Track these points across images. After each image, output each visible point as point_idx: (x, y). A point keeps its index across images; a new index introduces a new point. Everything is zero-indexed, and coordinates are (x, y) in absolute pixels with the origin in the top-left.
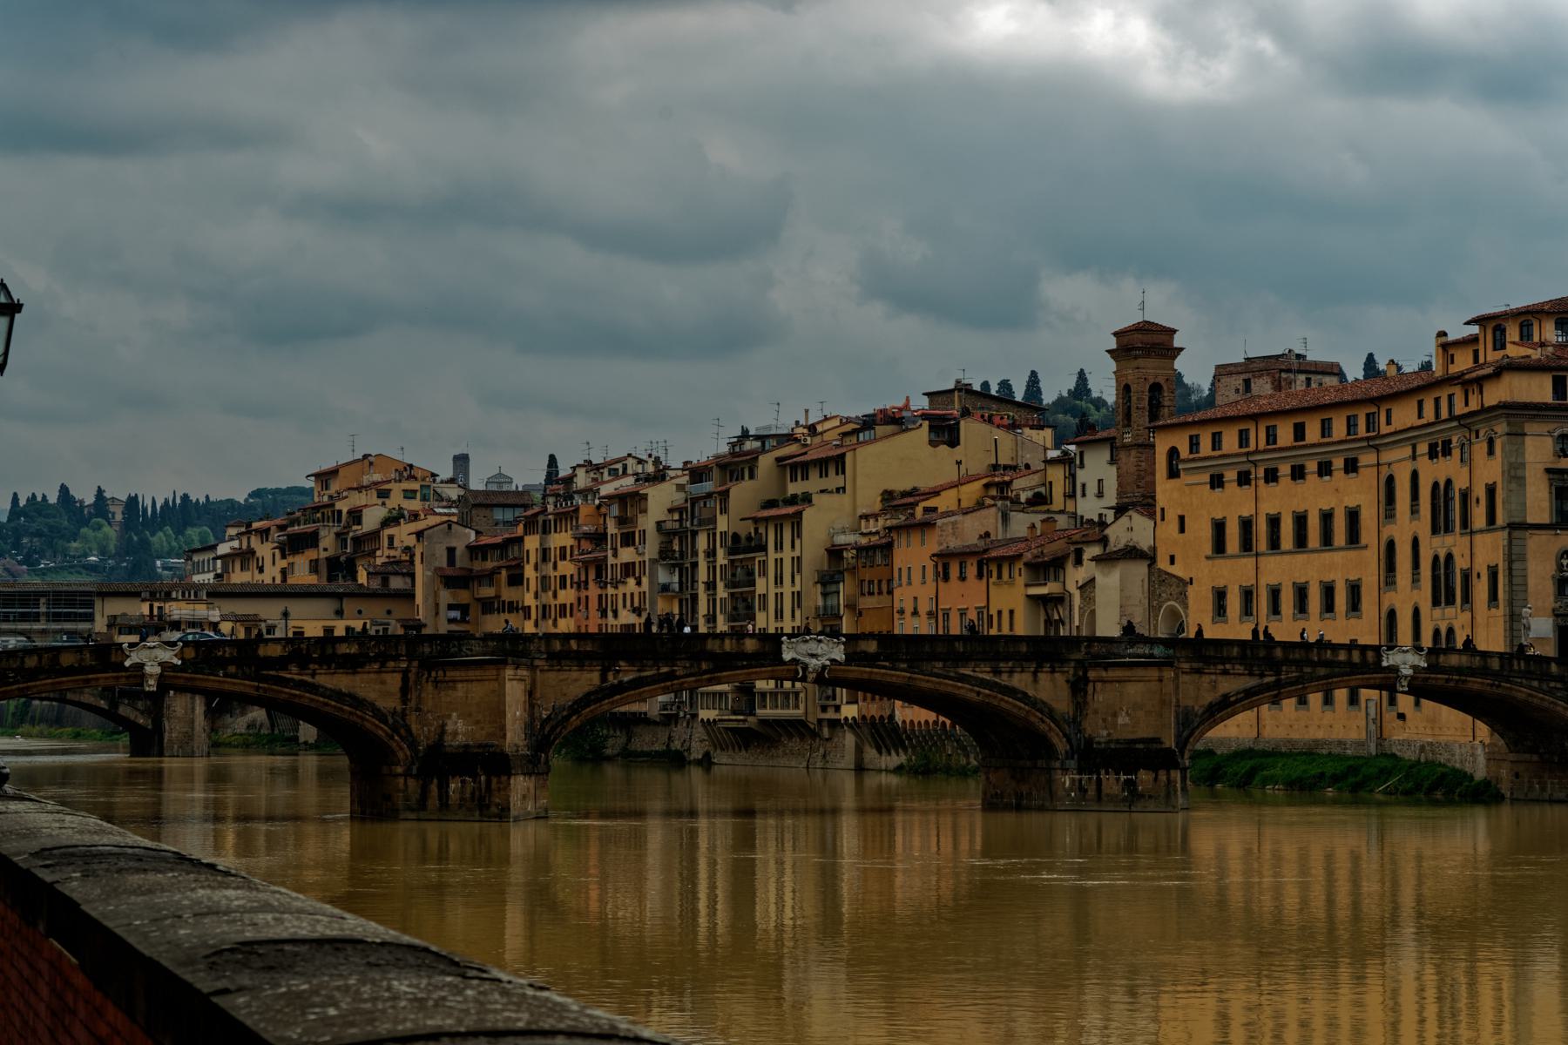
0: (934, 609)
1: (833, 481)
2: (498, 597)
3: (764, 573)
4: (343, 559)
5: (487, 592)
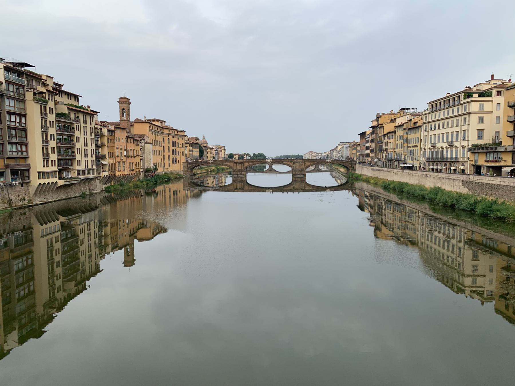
0: (126, 148)
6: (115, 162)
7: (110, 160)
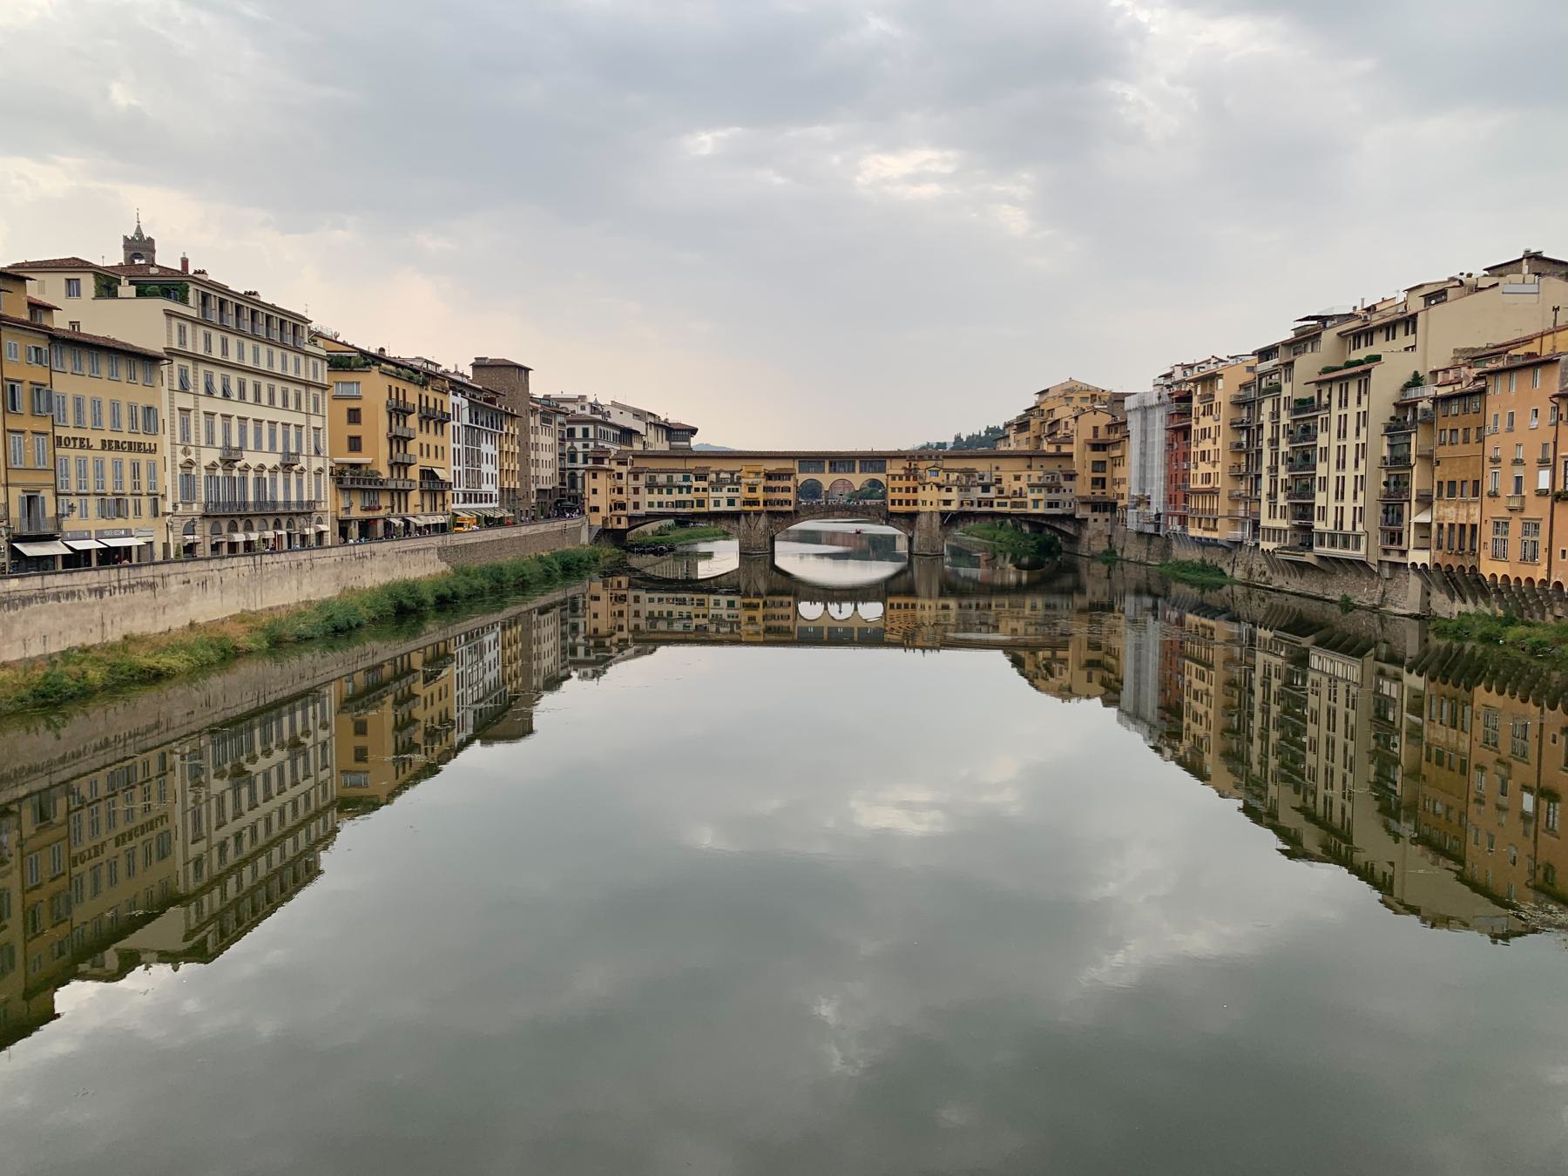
0: (1551, 456)
1: (1402, 339)
4: (1042, 437)
6: (1476, 520)
7: (1448, 510)
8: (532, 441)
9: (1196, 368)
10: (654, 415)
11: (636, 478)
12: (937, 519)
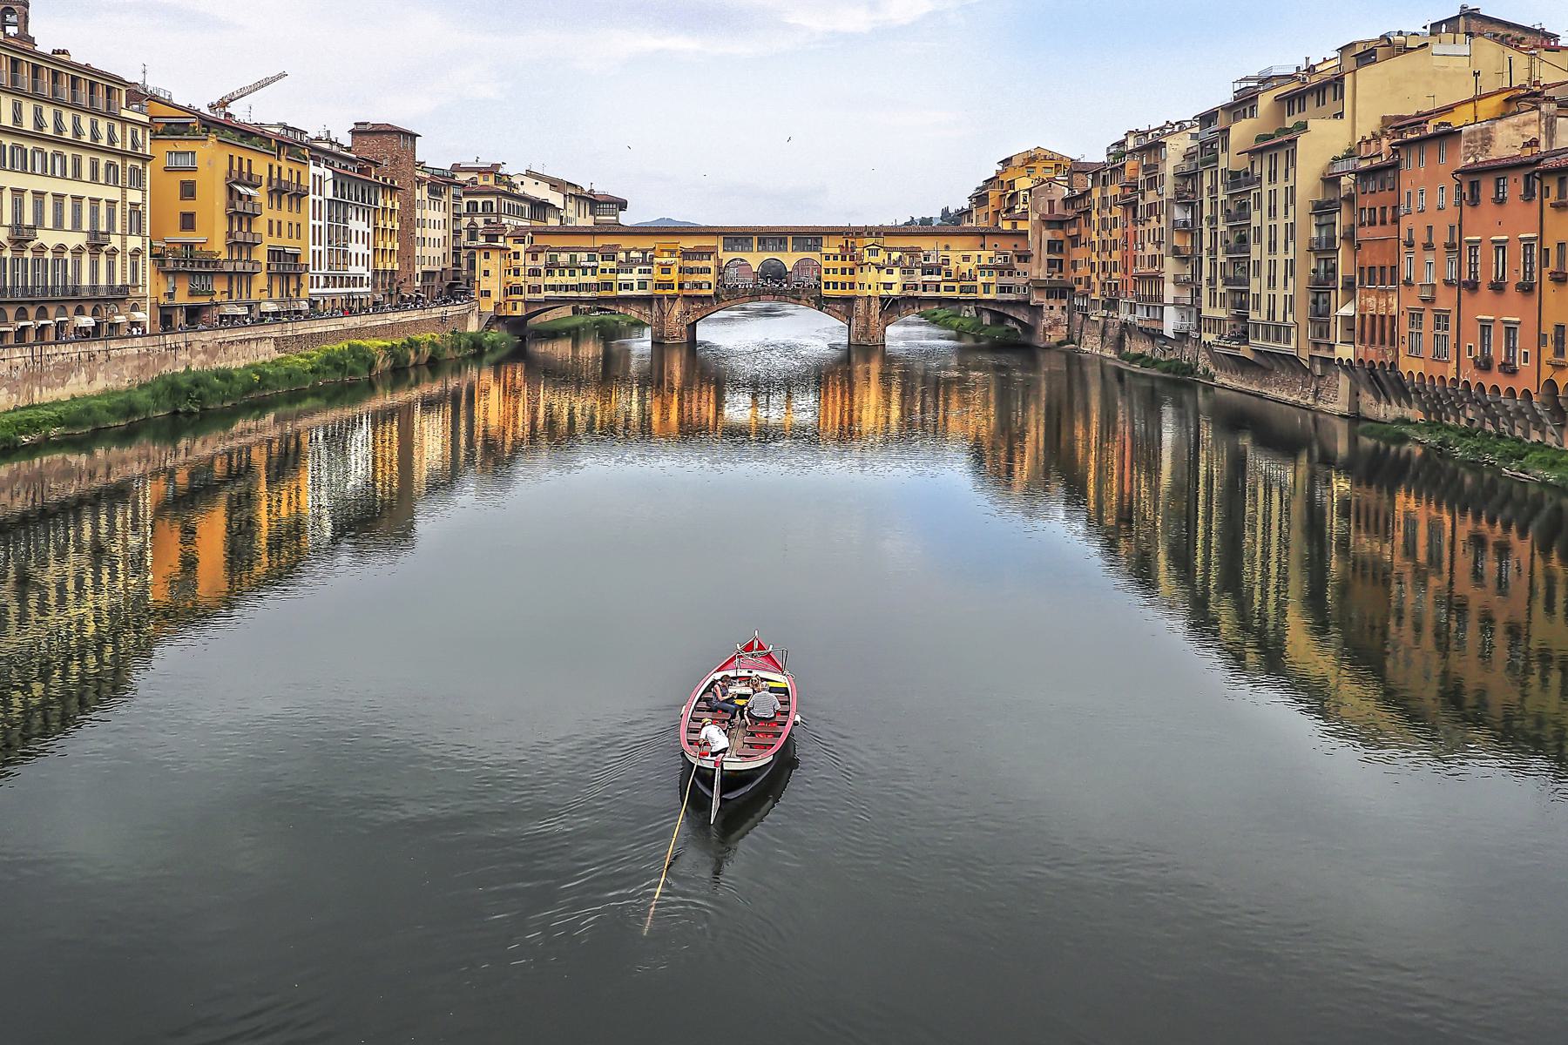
0: (1457, 241)
2: (1079, 235)
3: (1260, 207)
5: (1074, 231)
7: (1369, 300)
8: (418, 216)
9: (1150, 135)
10: (576, 186)
11: (535, 258)
12: (876, 307)
